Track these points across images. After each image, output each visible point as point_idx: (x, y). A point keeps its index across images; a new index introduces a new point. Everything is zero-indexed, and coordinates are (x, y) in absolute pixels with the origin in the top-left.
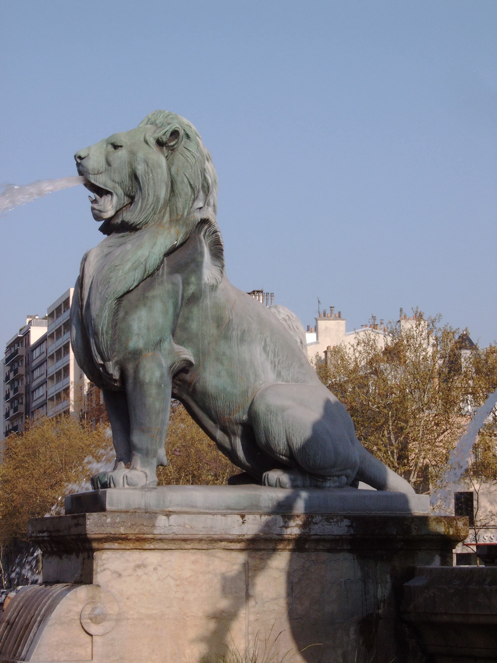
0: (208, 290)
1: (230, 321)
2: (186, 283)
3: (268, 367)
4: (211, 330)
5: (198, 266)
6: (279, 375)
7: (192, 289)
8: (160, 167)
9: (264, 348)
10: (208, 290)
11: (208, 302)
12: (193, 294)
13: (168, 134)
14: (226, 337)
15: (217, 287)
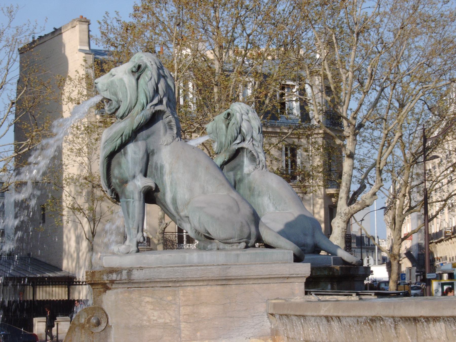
0: (246, 176)
1: (254, 188)
2: (235, 175)
3: (271, 205)
4: (248, 192)
5: (240, 166)
6: (276, 208)
7: (238, 177)
8: (222, 129)
9: (269, 198)
10: (246, 176)
11: (246, 181)
12: (240, 179)
13: (226, 115)
14: (253, 195)
15: (250, 174)
